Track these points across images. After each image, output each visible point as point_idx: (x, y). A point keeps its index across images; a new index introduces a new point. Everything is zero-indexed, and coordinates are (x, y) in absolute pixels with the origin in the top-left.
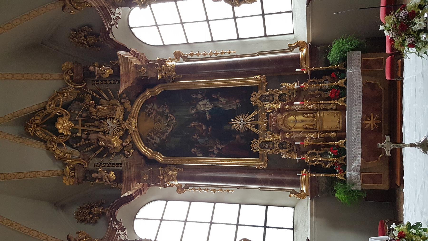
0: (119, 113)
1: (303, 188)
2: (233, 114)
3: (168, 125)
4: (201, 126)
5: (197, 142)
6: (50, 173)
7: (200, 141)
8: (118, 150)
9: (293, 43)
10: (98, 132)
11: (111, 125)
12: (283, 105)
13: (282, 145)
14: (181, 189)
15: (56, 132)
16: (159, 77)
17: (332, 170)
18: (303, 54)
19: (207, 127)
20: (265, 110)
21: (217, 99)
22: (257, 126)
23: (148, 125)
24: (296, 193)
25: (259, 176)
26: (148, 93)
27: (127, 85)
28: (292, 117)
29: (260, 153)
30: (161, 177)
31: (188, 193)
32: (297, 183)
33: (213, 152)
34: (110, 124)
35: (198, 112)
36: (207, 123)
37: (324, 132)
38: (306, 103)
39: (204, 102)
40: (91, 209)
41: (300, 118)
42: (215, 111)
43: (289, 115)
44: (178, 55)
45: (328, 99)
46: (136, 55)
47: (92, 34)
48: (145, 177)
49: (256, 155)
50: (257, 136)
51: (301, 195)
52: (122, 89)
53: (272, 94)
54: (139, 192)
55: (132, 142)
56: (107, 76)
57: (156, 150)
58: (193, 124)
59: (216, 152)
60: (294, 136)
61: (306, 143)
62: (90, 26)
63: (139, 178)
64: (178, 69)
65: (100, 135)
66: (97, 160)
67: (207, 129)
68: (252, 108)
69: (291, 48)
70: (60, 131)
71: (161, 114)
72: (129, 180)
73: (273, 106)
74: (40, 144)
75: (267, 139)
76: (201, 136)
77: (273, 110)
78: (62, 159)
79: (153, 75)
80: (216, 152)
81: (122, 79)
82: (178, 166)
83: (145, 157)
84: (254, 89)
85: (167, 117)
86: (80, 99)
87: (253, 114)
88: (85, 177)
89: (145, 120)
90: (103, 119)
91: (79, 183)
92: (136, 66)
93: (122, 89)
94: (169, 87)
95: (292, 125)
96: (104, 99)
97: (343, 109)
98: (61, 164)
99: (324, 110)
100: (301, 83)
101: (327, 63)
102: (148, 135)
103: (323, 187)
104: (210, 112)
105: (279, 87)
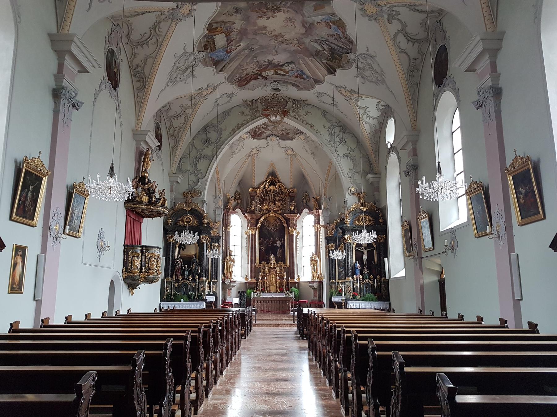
0: (276, 209)
1: (250, 280)
2: (275, 255)
3: (271, 229)
4: (271, 242)
5: (265, 240)
6: (254, 183)
7: (266, 241)
8: (262, 208)
9: (300, 276)
10: (269, 200)
11: (272, 206)
12: (278, 273)
13: (264, 273)
14: (246, 233)
15: (270, 185)
16: (290, 228)
17: (257, 289)
18: (295, 280)
19: (271, 245)
20: (277, 267)
21: (281, 249)
22: (271, 264)
23: (272, 221)
24: (247, 277)
25: (253, 265)
26: (284, 221)
27: (287, 216)
28: (274, 276)
29: (261, 265)
30: (252, 228)
31: (245, 236)
32: (251, 278)
33: (261, 247)
34: (272, 206)
35: (276, 241)
36: (272, 245)
37: (269, 287)
38: (279, 281)
39: (280, 243)
40: (240, 198)
41: (274, 279)
42: (277, 248)
43: (275, 275)
44: (298, 233)
45: (280, 288)
46: (299, 217)
47: (306, 202)
48: (253, 222)
49: (260, 263)
50: (268, 263)
51: (246, 279)
52: (285, 215)
53: (282, 269)
54: (246, 217)
55: (265, 214)
56: (291, 208)
57: (262, 223)
58: (272, 239)
59: (261, 248)
60: (267, 277)
61: (266, 281)
62: (309, 201)
63: (252, 218)
64: (293, 235)
65: (268, 202)
66: (258, 199)
67: (270, 244)
68: (277, 262)
69: (298, 276)
70: (270, 187)
71: (276, 226)
72: (251, 216)
73: (278, 270)
74: (265, 179)
75: (266, 268)
76: (267, 242)
77: (277, 270)
78: (259, 187)
79: (290, 225)
80: (261, 248)
81: (289, 215)
82: (255, 233)
83: (259, 219)
84: (284, 263)
85: (275, 228)
86: (282, 193)
87: (275, 263)
88: (252, 196)
89: (274, 219)
90: (274, 202)
91: (250, 194)
92: (294, 219)
93: (285, 215)
94: (286, 229)
95: (271, 276)
96: (282, 203)
97: (277, 292)
98: (257, 186)
99: (276, 287)
100: (286, 279)
101: (291, 287)
102: (268, 220)
103: (251, 286)
104: (276, 246)
105: (284, 272)
